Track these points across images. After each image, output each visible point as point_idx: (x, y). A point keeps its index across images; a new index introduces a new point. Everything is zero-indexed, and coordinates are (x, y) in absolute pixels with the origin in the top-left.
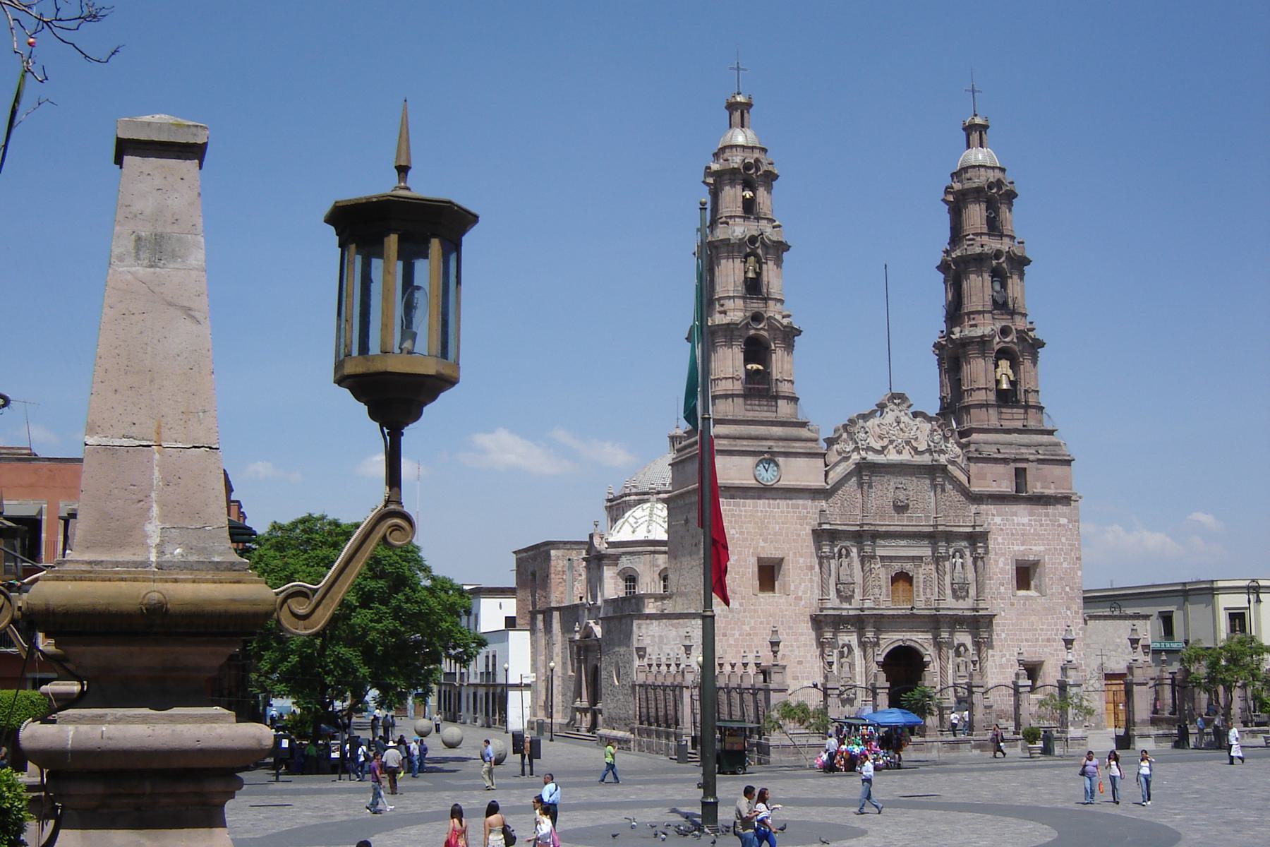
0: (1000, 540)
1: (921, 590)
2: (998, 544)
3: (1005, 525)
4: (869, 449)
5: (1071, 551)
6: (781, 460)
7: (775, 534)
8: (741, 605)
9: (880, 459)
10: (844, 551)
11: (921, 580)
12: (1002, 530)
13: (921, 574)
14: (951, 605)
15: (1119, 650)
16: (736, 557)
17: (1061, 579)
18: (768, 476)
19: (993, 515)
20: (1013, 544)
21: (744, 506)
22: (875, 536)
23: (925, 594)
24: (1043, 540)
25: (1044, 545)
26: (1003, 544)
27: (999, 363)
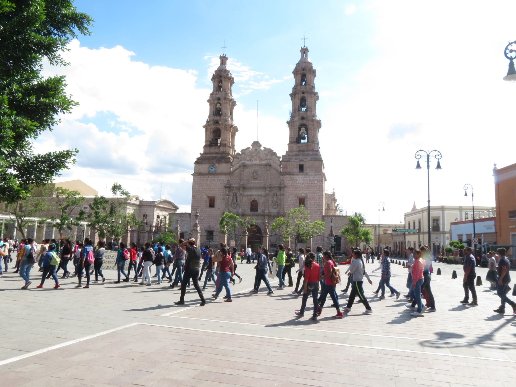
0: (291, 189)
1: (261, 206)
2: (290, 190)
3: (293, 184)
4: (245, 159)
5: (319, 192)
6: (217, 165)
7: (213, 189)
8: (201, 210)
9: (249, 163)
10: (235, 194)
11: (261, 203)
12: (292, 186)
13: (261, 201)
14: (274, 211)
15: (337, 229)
16: (200, 196)
17: (315, 202)
18: (212, 170)
19: (289, 181)
20: (296, 191)
21: (204, 180)
22: (245, 188)
23: (262, 207)
24: (307, 189)
25: (308, 190)
26: (292, 190)
27: (301, 129)
